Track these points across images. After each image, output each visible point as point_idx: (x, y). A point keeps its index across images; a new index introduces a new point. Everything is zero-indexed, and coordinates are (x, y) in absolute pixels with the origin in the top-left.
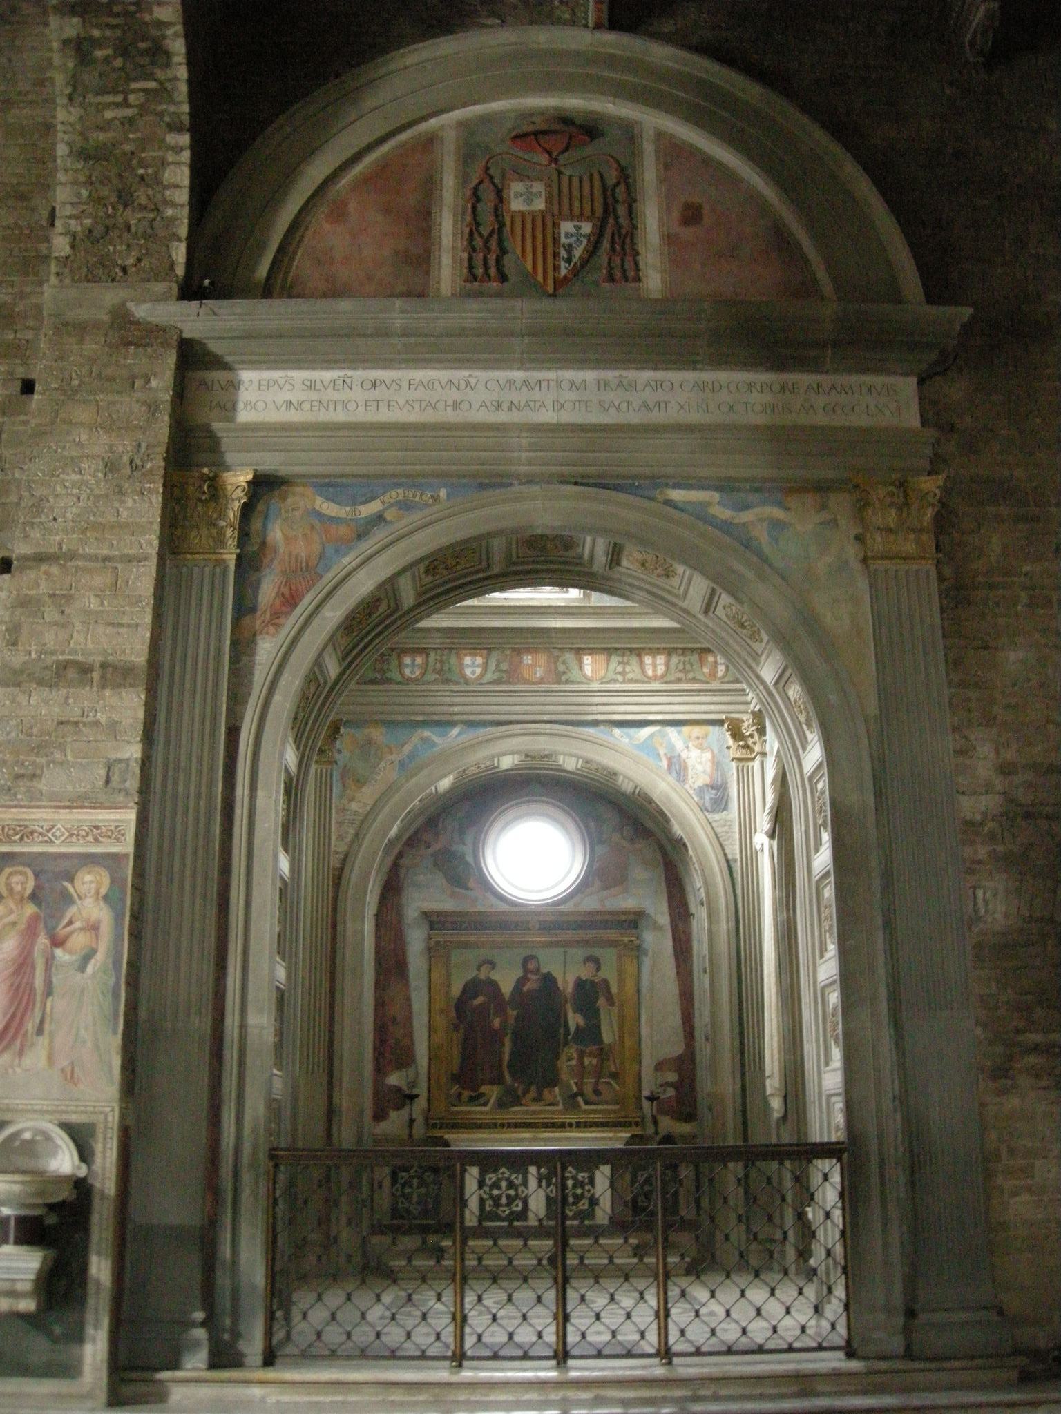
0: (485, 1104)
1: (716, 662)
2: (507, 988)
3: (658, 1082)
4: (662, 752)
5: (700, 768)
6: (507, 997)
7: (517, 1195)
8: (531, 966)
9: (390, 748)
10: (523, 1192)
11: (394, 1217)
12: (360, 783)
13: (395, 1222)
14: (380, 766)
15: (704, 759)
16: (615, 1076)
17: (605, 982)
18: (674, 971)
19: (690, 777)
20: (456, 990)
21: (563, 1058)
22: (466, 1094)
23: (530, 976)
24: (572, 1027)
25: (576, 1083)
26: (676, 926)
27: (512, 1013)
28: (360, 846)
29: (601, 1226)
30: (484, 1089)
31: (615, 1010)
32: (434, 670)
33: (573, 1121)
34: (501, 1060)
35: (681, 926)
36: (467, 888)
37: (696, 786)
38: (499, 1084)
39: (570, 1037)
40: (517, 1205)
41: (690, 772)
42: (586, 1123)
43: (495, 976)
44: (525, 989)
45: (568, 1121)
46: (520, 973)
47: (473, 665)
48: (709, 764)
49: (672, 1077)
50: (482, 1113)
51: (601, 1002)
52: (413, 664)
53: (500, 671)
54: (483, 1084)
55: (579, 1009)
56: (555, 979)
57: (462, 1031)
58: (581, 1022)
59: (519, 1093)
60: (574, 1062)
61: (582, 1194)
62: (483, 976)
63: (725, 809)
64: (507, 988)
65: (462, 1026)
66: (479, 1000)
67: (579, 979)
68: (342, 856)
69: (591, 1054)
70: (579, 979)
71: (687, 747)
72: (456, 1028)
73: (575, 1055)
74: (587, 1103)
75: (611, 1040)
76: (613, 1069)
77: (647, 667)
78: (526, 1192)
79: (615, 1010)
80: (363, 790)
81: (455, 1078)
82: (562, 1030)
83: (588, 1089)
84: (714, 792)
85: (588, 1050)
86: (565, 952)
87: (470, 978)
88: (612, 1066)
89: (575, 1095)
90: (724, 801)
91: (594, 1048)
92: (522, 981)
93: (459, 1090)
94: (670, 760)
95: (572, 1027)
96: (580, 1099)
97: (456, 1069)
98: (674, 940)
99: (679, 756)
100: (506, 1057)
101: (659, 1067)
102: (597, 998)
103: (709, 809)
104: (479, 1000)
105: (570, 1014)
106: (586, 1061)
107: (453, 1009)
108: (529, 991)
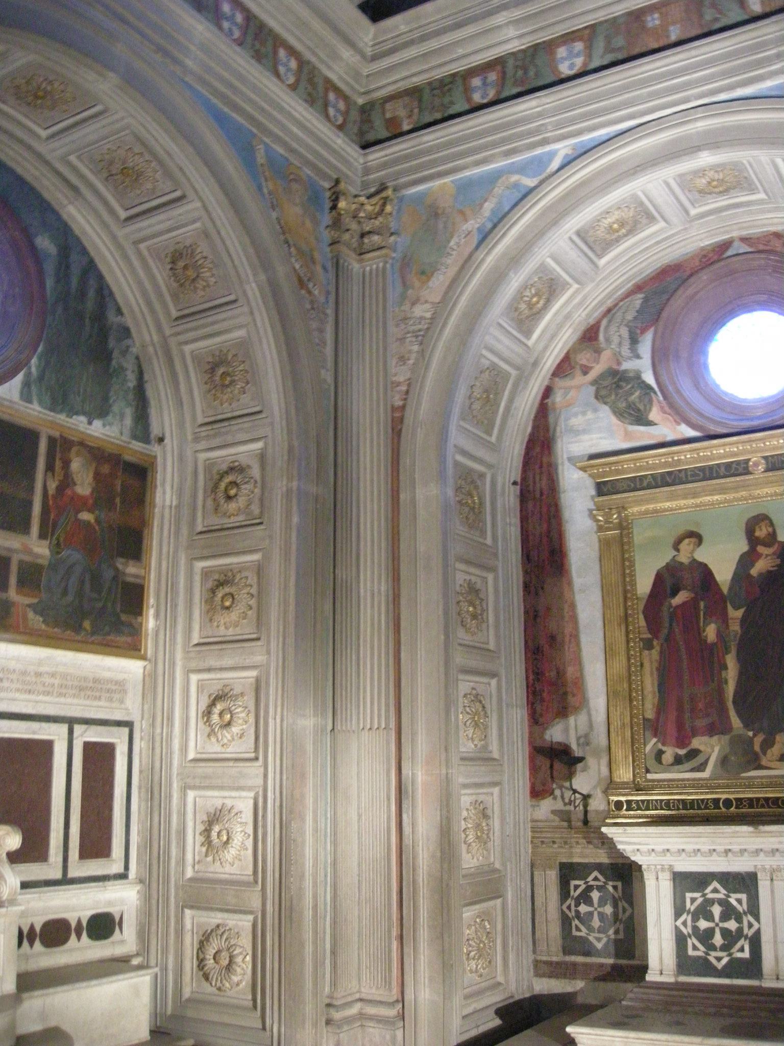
0: (701, 768)
2: (724, 574)
6: (725, 590)
7: (740, 930)
8: (761, 532)
9: (462, 212)
10: (750, 926)
11: (566, 951)
12: (426, 274)
13: (568, 958)
14: (452, 243)
20: (644, 585)
22: (669, 753)
23: (760, 549)
27: (736, 614)
28: (427, 368)
30: (697, 743)
32: (516, 81)
34: (721, 692)
36: (650, 423)
38: (723, 733)
40: (742, 950)
43: (702, 555)
44: (754, 572)
46: (744, 547)
47: (571, 55)
50: (696, 785)
52: (485, 84)
53: (613, 50)
54: (695, 733)
57: (658, 648)
59: (757, 748)
62: (684, 558)
64: (724, 574)
65: (655, 643)
66: (680, 598)
68: (404, 388)
72: (648, 645)
78: (756, 925)
80: (430, 284)
81: (655, 727)
87: (664, 564)
92: (747, 560)
93: (660, 746)
97: (650, 715)
100: (730, 688)
104: (680, 598)
107: (641, 617)
108: (761, 574)
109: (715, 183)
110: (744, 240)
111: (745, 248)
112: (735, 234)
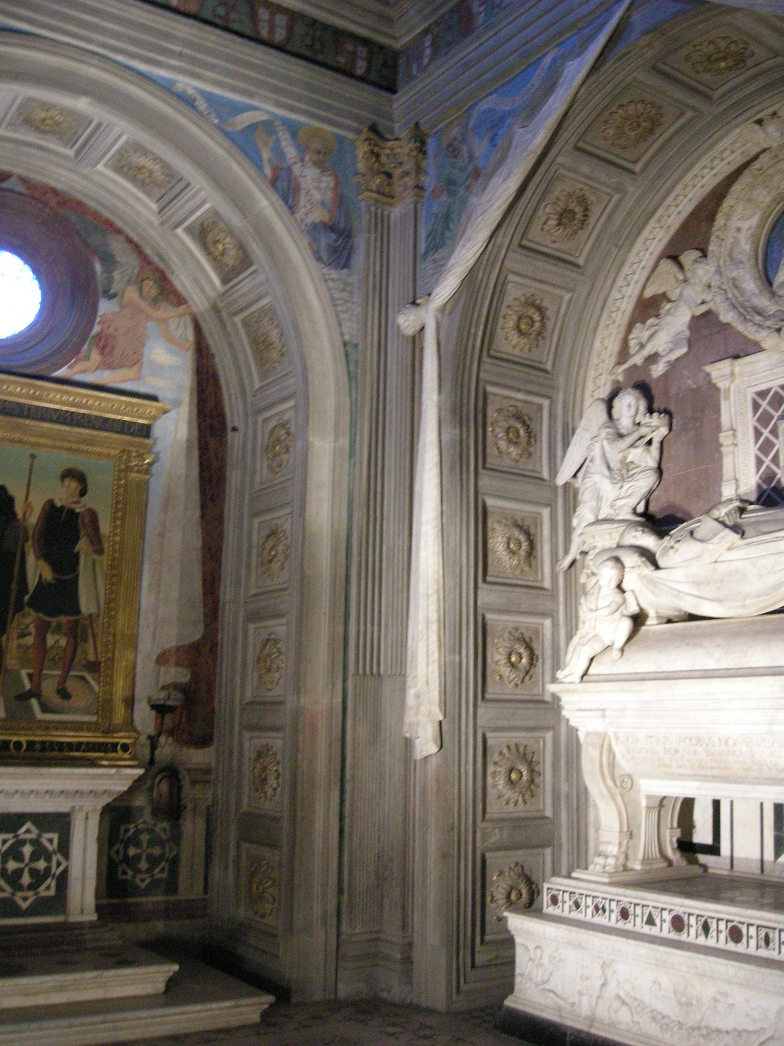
1: (354, 53)
3: (161, 683)
4: (266, 155)
5: (317, 196)
15: (324, 185)
16: (94, 667)
17: (93, 515)
18: (198, 513)
19: (302, 204)
21: (14, 629)
24: (32, 582)
25: (30, 676)
26: (207, 443)
29: (80, 926)
31: (105, 560)
33: (23, 739)
35: (212, 443)
37: (309, 220)
39: (27, 598)
41: (303, 201)
42: (43, 743)
45: (15, 739)
48: (330, 194)
49: (182, 676)
51: (83, 546)
55: (46, 554)
56: (10, 501)
58: (48, 575)
60: (29, 640)
61: (48, 870)
63: (346, 266)
67: (50, 504)
69: (58, 629)
70: (50, 504)
71: (302, 160)
73: (32, 629)
74: (45, 709)
75: (93, 610)
76: (91, 657)
77: (261, 24)
79: (105, 560)
82: (14, 586)
83: (49, 687)
84: (334, 236)
85: (54, 621)
86: (33, 456)
88: (91, 651)
89: (24, 697)
90: (346, 253)
91: (64, 619)
94: (276, 170)
95: (32, 582)
96: (34, 702)
98: (201, 465)
99: (289, 169)
101: (162, 659)
102: (77, 539)
103: (325, 258)
105: (31, 559)
106: (51, 640)
109: (48, 122)
110: (24, 181)
111: (20, 188)
112: (17, 170)
